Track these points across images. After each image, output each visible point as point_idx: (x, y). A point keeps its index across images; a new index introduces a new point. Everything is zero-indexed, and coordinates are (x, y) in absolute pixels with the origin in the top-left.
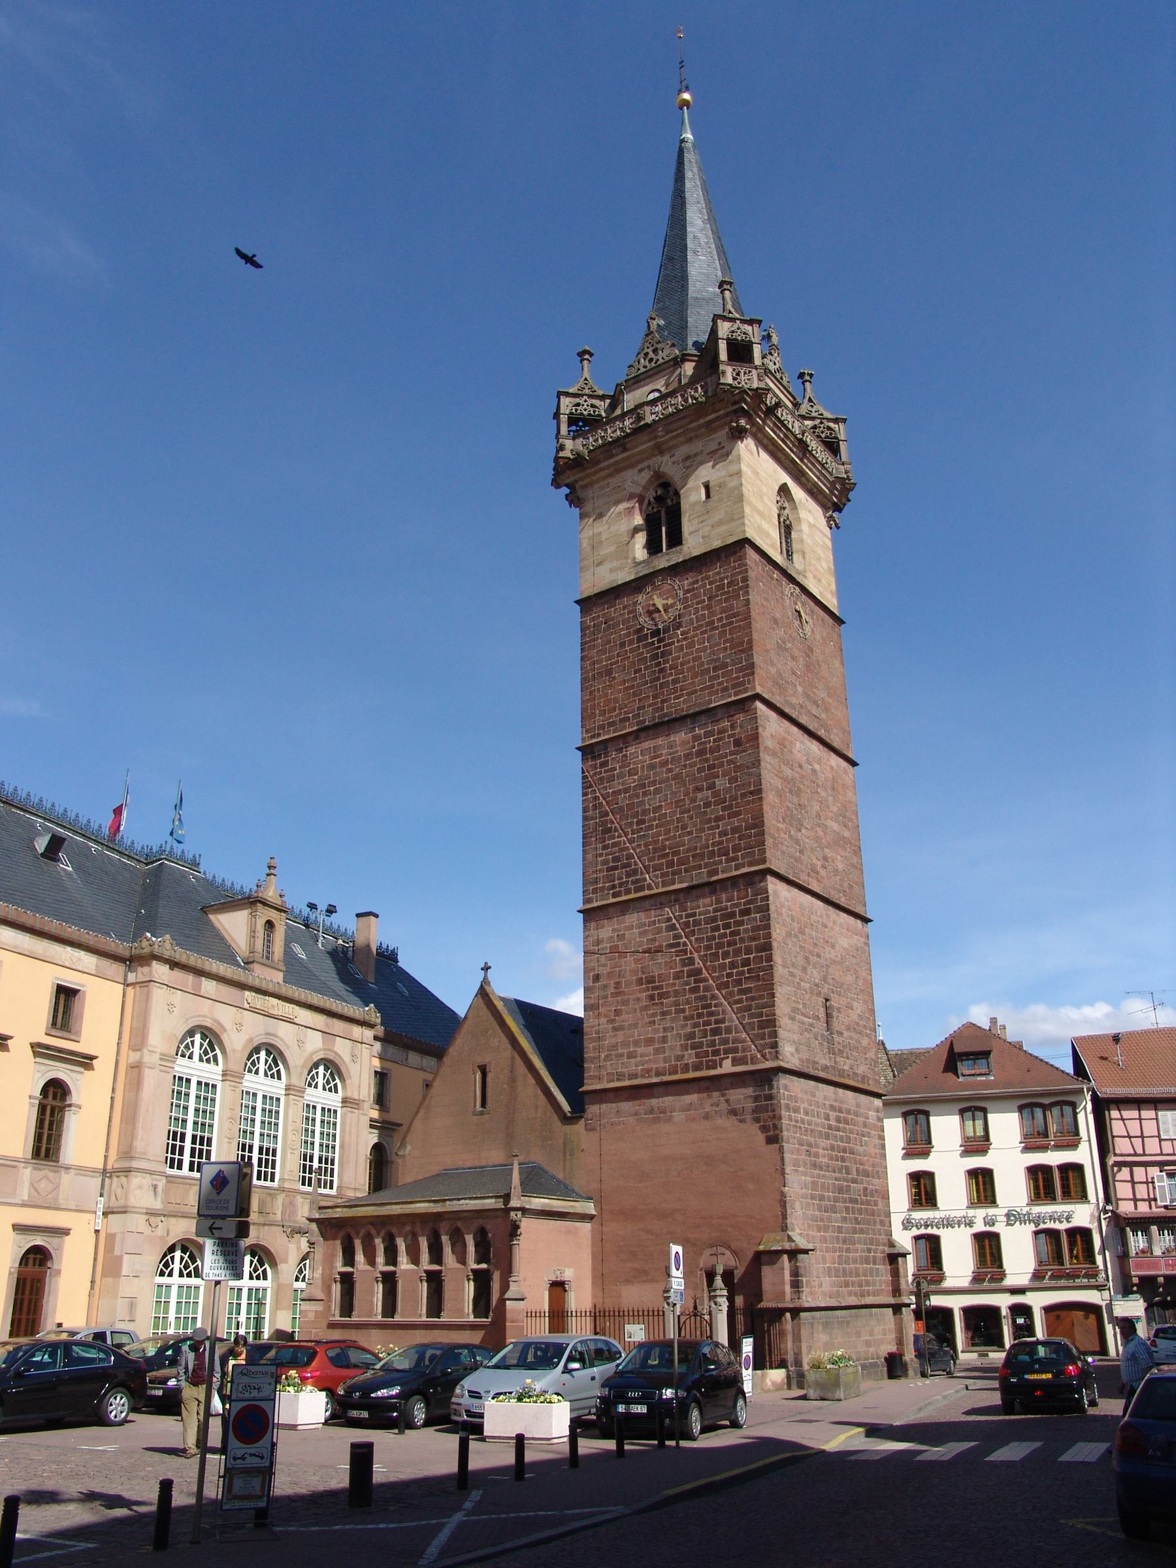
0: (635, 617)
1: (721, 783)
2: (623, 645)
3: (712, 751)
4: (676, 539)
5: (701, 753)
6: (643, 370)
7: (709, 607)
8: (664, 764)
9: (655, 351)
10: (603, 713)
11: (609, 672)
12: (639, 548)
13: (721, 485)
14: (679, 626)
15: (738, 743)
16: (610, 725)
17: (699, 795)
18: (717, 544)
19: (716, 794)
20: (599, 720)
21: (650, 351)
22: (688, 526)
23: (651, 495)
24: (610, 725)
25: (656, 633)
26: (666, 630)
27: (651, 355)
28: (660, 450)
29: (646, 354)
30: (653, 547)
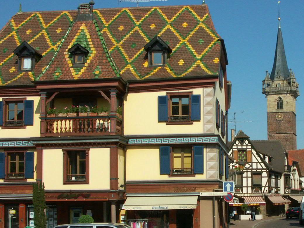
0: (276, 118)
1: (288, 143)
2: (274, 121)
3: (287, 138)
4: (282, 107)
5: (285, 138)
6: (277, 79)
7: (287, 119)
8: (280, 139)
9: (279, 77)
10: (271, 130)
11: (272, 124)
12: (276, 107)
13: (289, 102)
14: (282, 121)
15: (290, 138)
16: (272, 132)
17: (285, 144)
18: (288, 111)
19: (287, 144)
20: (270, 131)
21: (279, 76)
22: (284, 107)
23: (278, 99)
24: (272, 132)
25: (279, 121)
26: (281, 121)
27: (279, 77)
28: (280, 94)
29: (278, 77)
30: (278, 107)
